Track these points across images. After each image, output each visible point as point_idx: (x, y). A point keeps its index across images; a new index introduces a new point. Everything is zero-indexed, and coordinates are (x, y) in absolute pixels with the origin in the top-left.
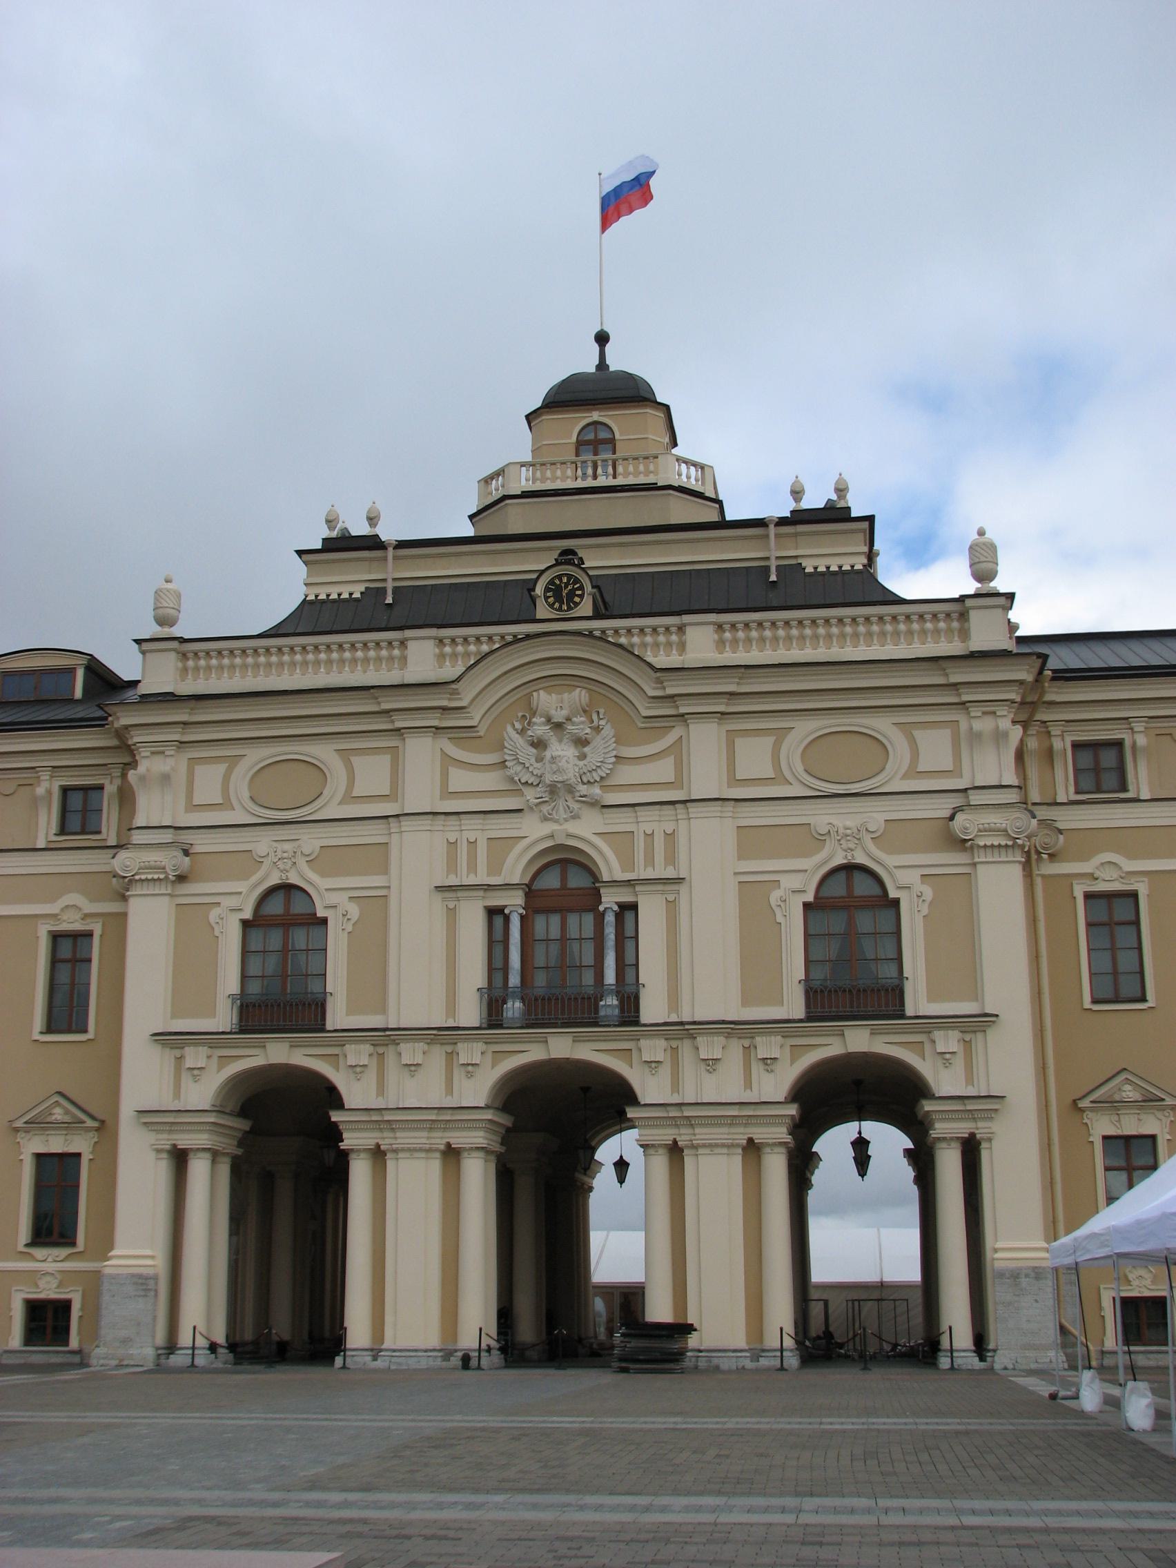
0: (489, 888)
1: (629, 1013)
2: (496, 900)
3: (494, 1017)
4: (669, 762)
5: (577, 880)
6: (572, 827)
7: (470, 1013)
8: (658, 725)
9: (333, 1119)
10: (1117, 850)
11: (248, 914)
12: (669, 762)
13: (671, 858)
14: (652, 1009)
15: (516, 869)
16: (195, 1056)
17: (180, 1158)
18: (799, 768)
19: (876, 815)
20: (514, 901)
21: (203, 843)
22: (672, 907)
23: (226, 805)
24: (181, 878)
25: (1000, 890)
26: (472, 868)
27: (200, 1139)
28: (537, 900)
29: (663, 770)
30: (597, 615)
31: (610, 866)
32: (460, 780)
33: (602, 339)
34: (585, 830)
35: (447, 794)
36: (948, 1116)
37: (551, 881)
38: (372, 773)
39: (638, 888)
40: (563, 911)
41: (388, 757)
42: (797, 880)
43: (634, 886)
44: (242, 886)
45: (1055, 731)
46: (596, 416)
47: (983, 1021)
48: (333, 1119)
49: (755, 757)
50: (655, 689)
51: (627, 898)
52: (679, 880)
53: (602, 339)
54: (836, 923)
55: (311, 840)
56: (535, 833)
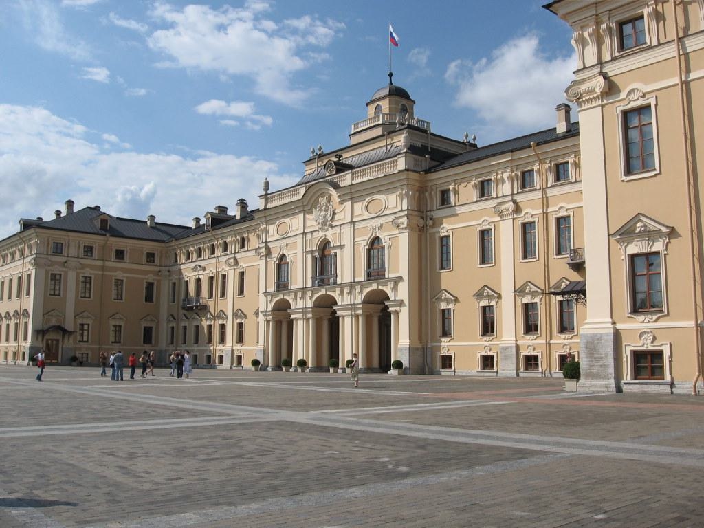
1: (335, 283)
3: (313, 285)
4: (343, 212)
6: (327, 233)
7: (309, 285)
8: (342, 202)
10: (488, 216)
13: (342, 240)
14: (339, 281)
16: (269, 297)
17: (268, 321)
19: (378, 222)
21: (270, 245)
22: (342, 253)
25: (403, 240)
27: (270, 318)
30: (337, 173)
33: (391, 75)
34: (329, 234)
36: (393, 306)
42: (363, 242)
45: (434, 187)
46: (378, 103)
47: (401, 279)
52: (344, 245)
53: (391, 75)
56: (321, 234)
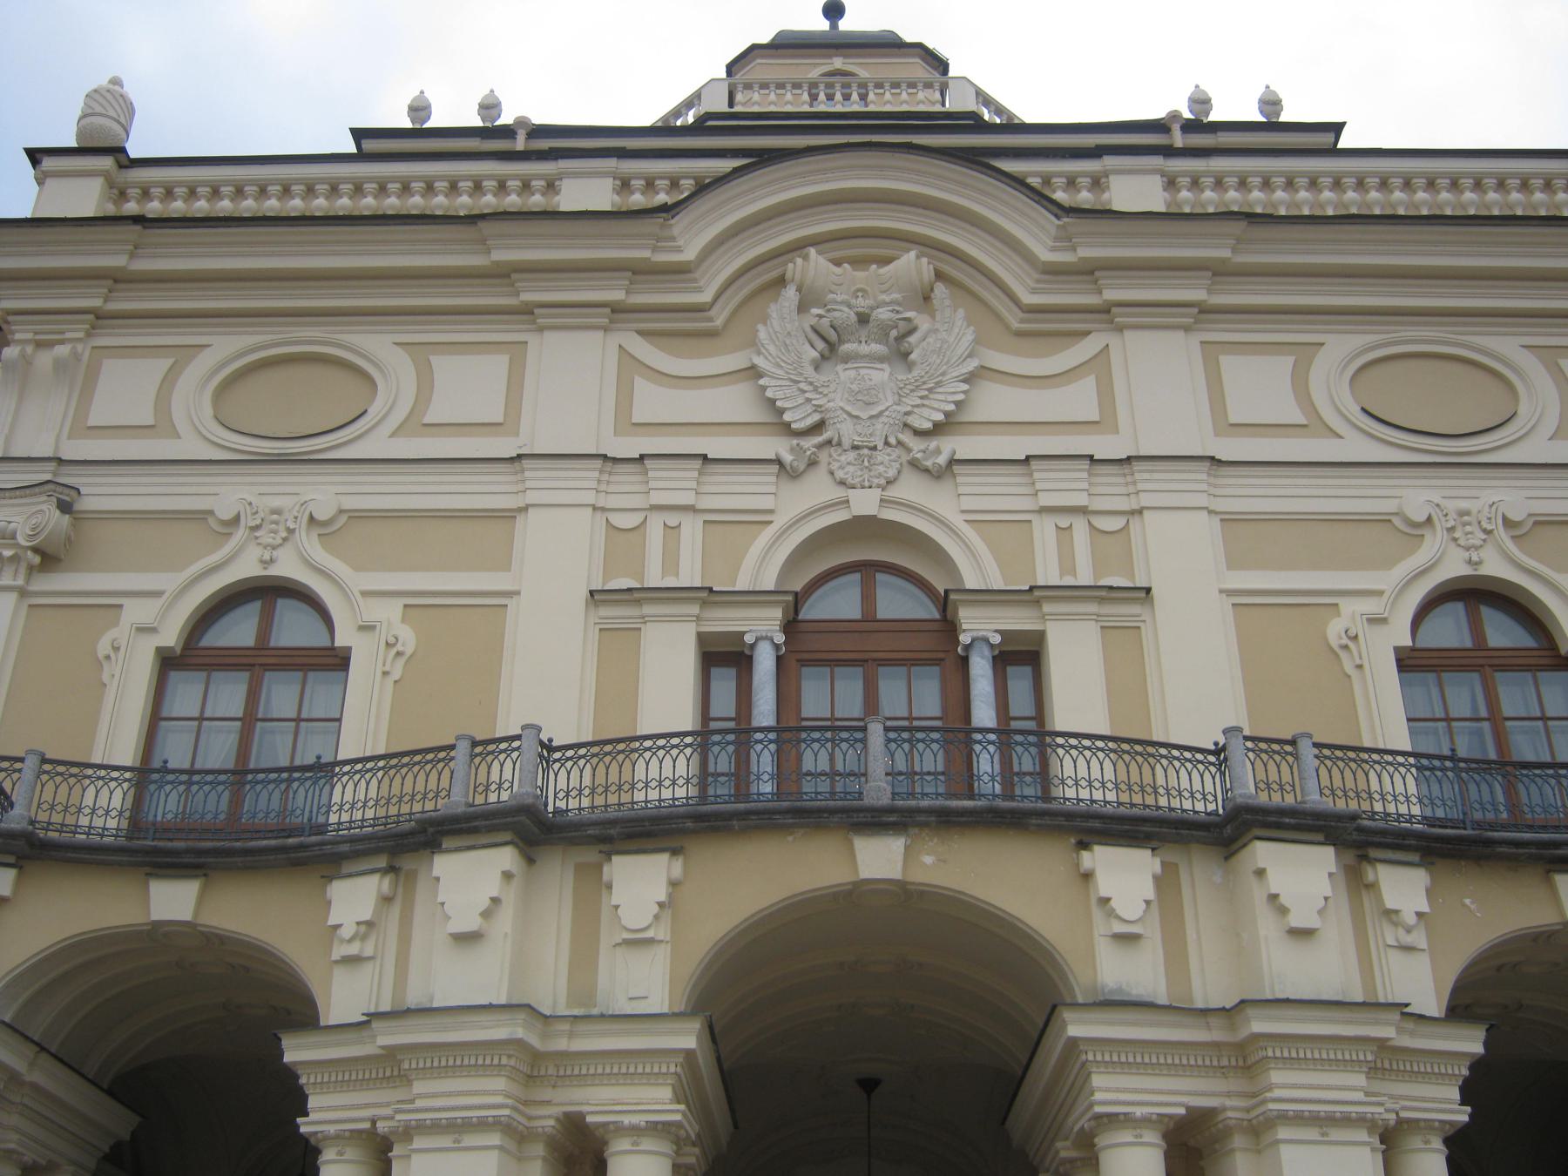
0: (708, 596)
2: (724, 621)
4: (1088, 384)
5: (896, 603)
9: (288, 1058)
11: (170, 637)
12: (1088, 384)
15: (762, 564)
18: (1354, 410)
20: (762, 628)
21: (98, 494)
23: (162, 425)
24: (48, 558)
26: (671, 561)
28: (804, 646)
29: (1079, 400)
31: (977, 567)
32: (652, 402)
35: (627, 424)
37: (840, 603)
38: (468, 384)
39: (1047, 608)
40: (869, 665)
41: (505, 359)
43: (1037, 602)
44: (168, 581)
48: (288, 1058)
49: (1259, 385)
50: (1034, 291)
51: (1018, 620)
54: (1463, 695)
55: (324, 494)
